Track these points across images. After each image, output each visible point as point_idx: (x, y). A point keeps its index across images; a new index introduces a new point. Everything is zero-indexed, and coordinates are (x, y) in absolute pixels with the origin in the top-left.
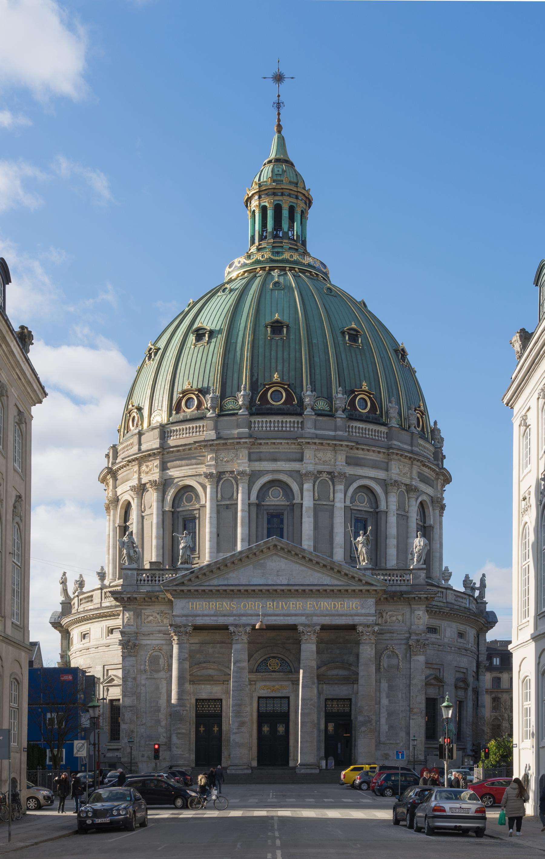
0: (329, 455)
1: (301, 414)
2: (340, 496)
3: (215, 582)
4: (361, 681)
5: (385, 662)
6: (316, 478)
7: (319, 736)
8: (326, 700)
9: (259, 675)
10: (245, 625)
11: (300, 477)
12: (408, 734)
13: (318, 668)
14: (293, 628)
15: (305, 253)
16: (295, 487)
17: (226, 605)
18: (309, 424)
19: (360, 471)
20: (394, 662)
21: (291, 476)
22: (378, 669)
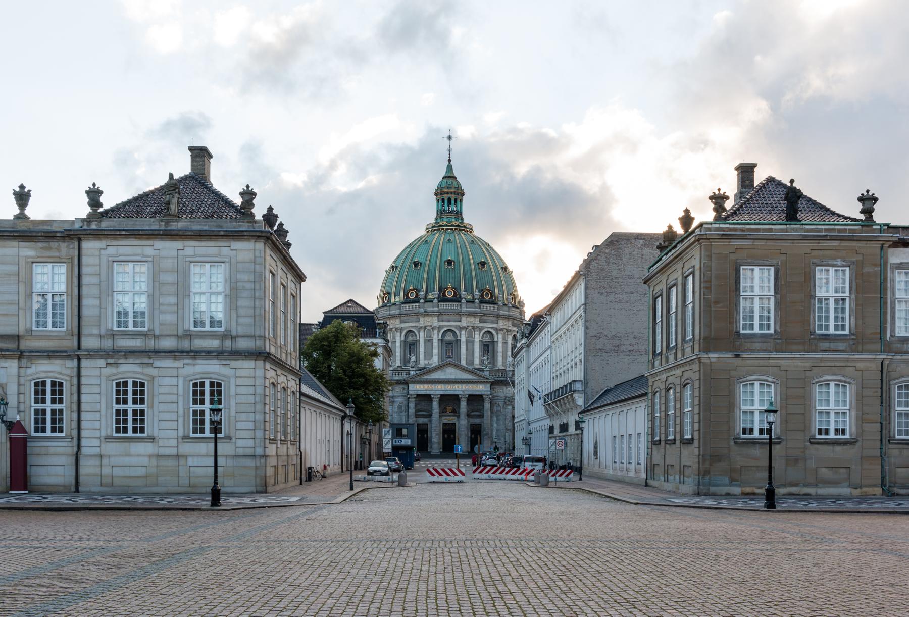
0: (471, 319)
1: (460, 302)
2: (477, 336)
3: (425, 377)
4: (485, 417)
5: (495, 409)
6: (467, 328)
7: (468, 439)
8: (471, 424)
9: (443, 414)
10: (438, 395)
11: (460, 329)
12: (505, 439)
13: (468, 411)
14: (458, 395)
15: (462, 219)
16: (458, 333)
17: (430, 387)
18: (464, 306)
19: (485, 325)
20: (499, 409)
21: (456, 328)
22: (492, 412)
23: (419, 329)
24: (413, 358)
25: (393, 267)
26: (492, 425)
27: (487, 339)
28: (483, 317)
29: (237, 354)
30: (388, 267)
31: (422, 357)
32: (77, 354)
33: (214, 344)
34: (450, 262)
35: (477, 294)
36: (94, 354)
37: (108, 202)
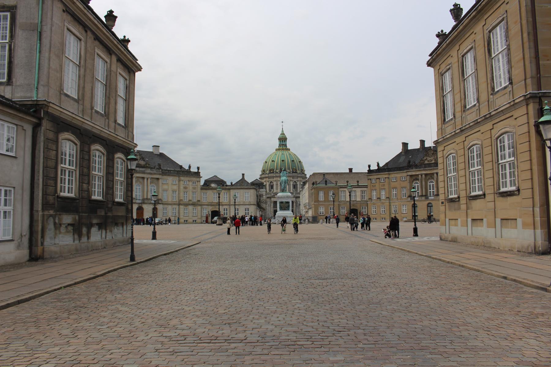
15: (287, 147)
23: (274, 181)
24: (272, 190)
25: (266, 162)
26: (296, 210)
27: (295, 184)
28: (293, 177)
29: (251, 205)
30: (264, 162)
31: (275, 189)
32: (230, 205)
33: (248, 203)
34: (283, 161)
35: (291, 170)
36: (232, 205)
37: (233, 184)
